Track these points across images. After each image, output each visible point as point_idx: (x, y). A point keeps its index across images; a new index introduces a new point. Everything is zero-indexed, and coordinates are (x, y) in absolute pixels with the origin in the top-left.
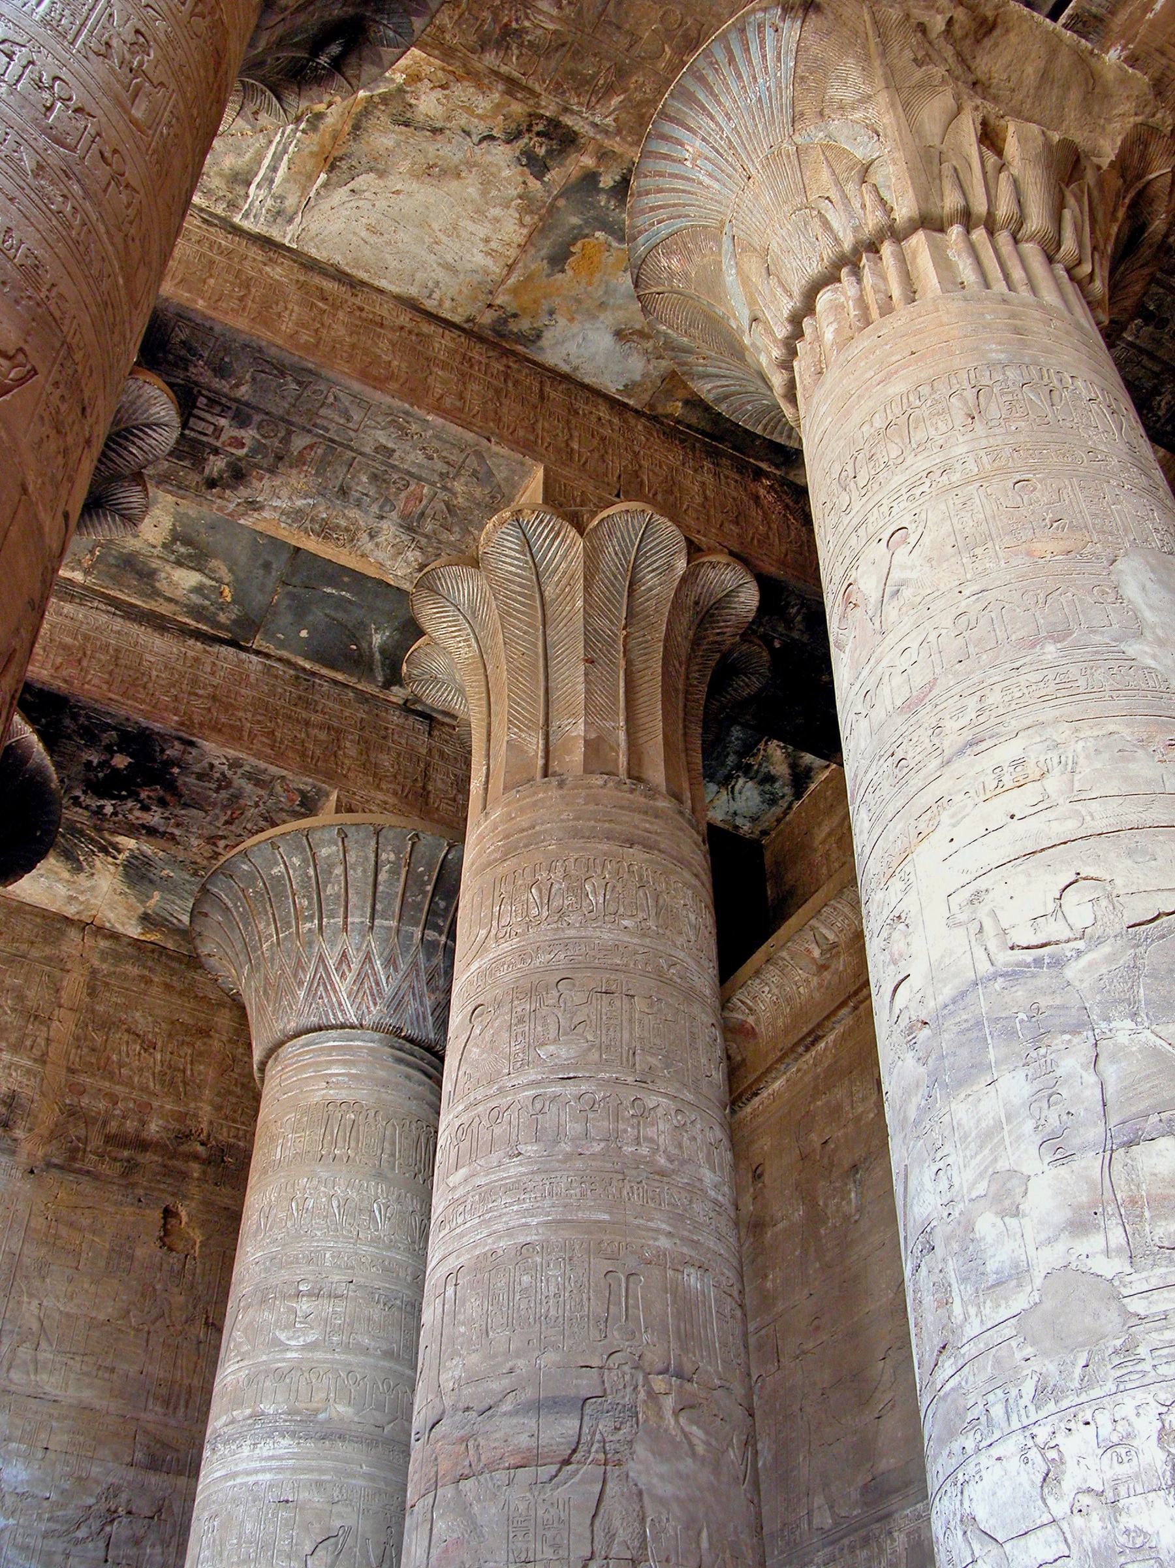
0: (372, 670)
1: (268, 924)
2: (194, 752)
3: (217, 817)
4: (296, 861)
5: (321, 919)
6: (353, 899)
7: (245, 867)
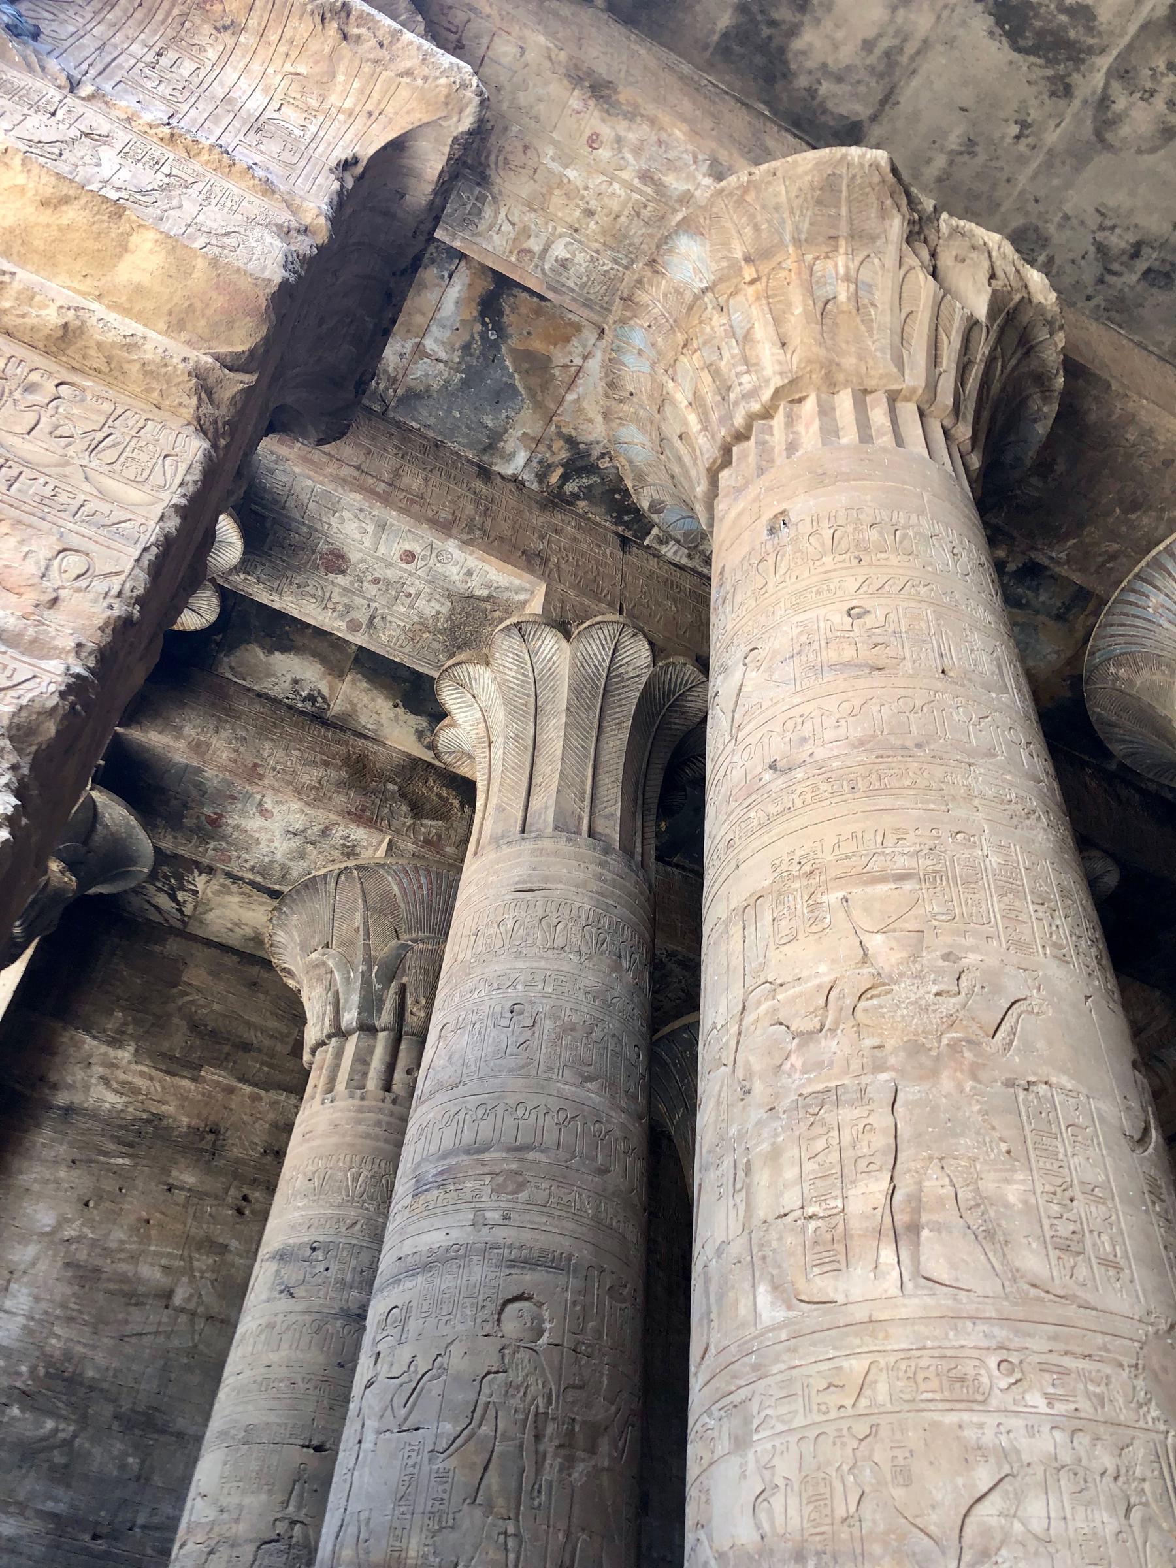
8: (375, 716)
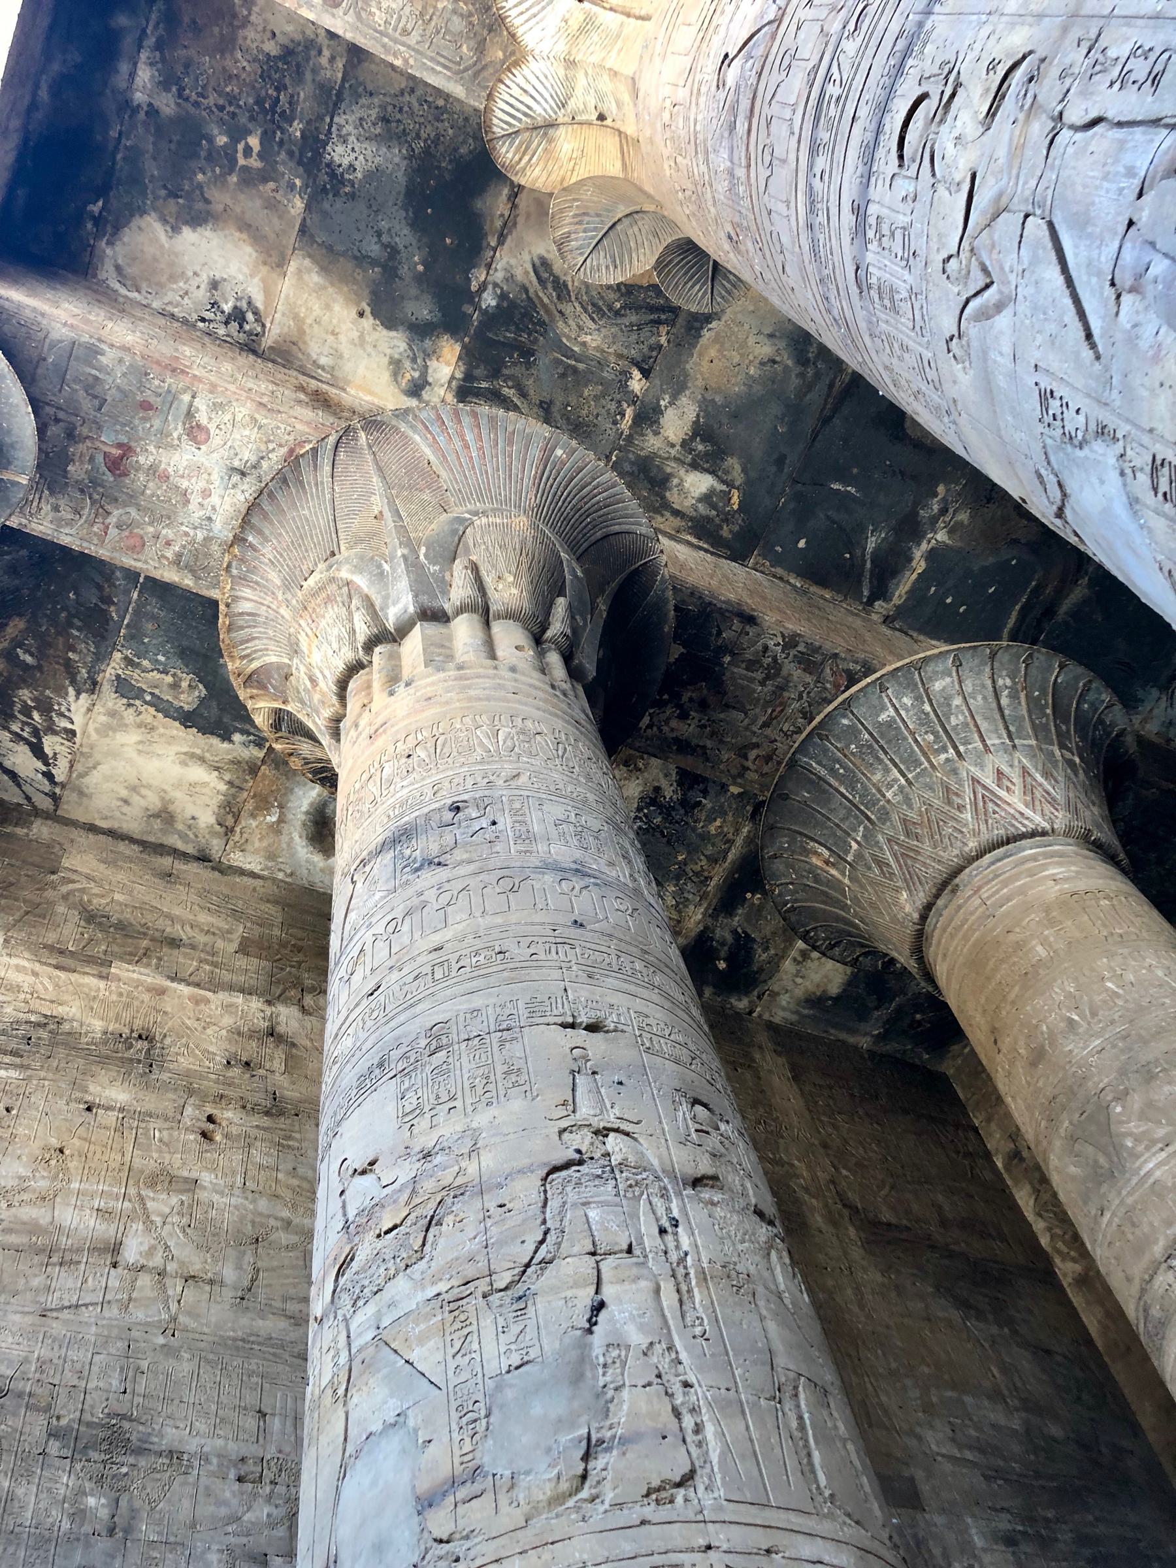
0: (860, 582)
1: (887, 771)
2: (752, 631)
3: (753, 722)
4: (907, 701)
5: (955, 748)
6: (984, 726)
7: (845, 722)
8: (331, 338)
